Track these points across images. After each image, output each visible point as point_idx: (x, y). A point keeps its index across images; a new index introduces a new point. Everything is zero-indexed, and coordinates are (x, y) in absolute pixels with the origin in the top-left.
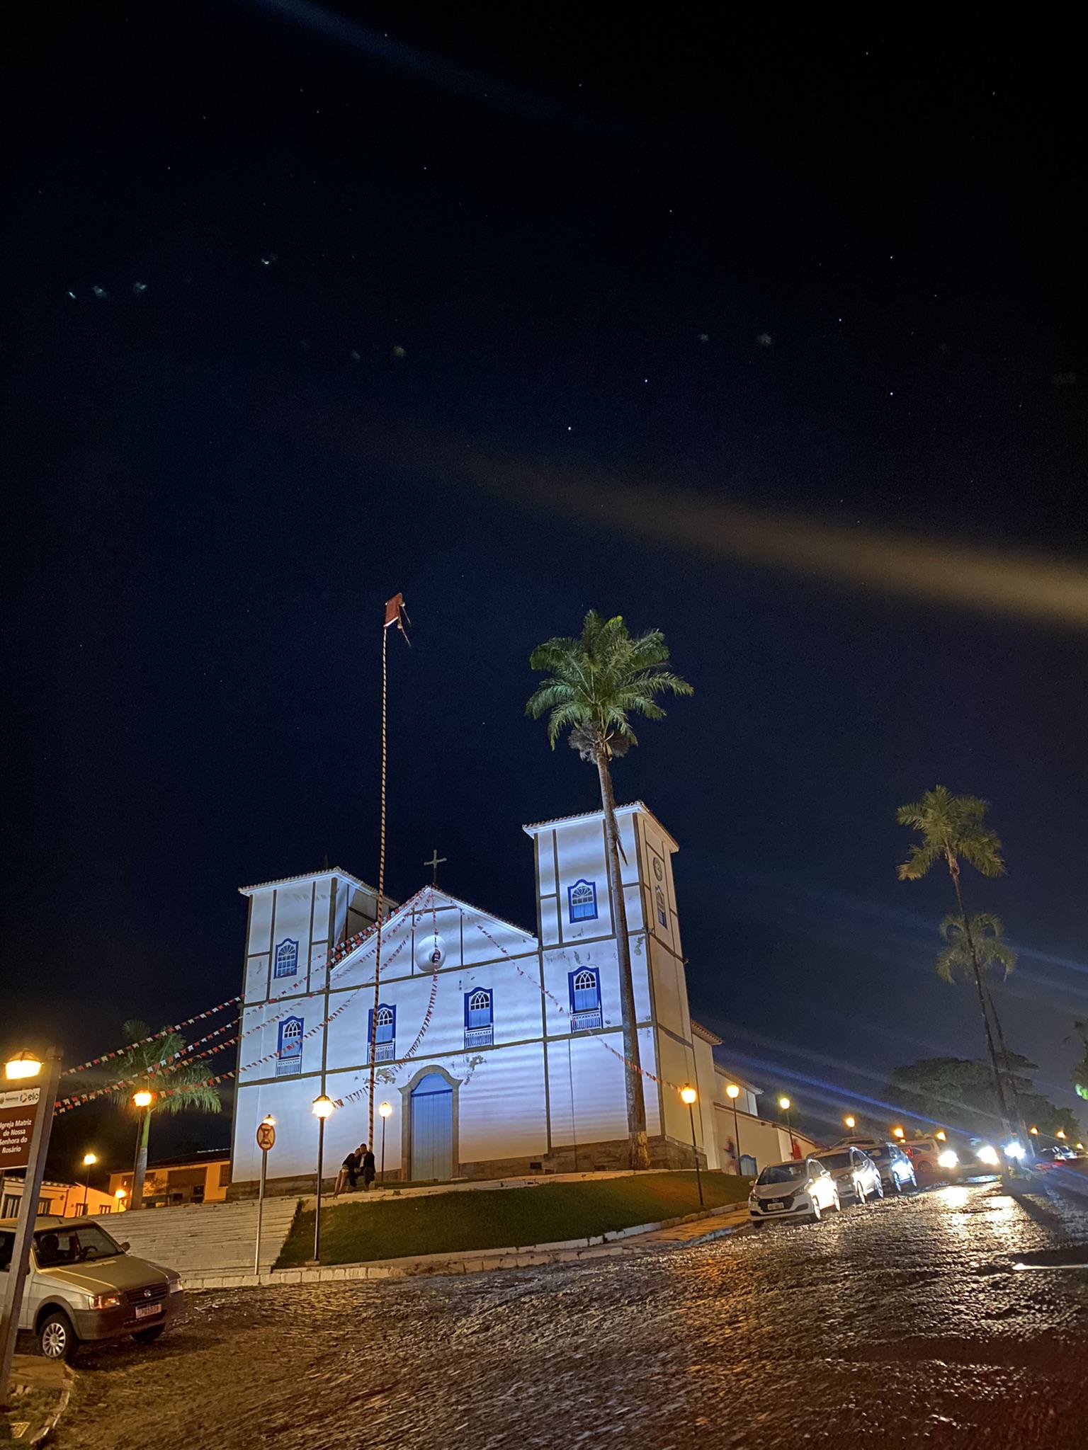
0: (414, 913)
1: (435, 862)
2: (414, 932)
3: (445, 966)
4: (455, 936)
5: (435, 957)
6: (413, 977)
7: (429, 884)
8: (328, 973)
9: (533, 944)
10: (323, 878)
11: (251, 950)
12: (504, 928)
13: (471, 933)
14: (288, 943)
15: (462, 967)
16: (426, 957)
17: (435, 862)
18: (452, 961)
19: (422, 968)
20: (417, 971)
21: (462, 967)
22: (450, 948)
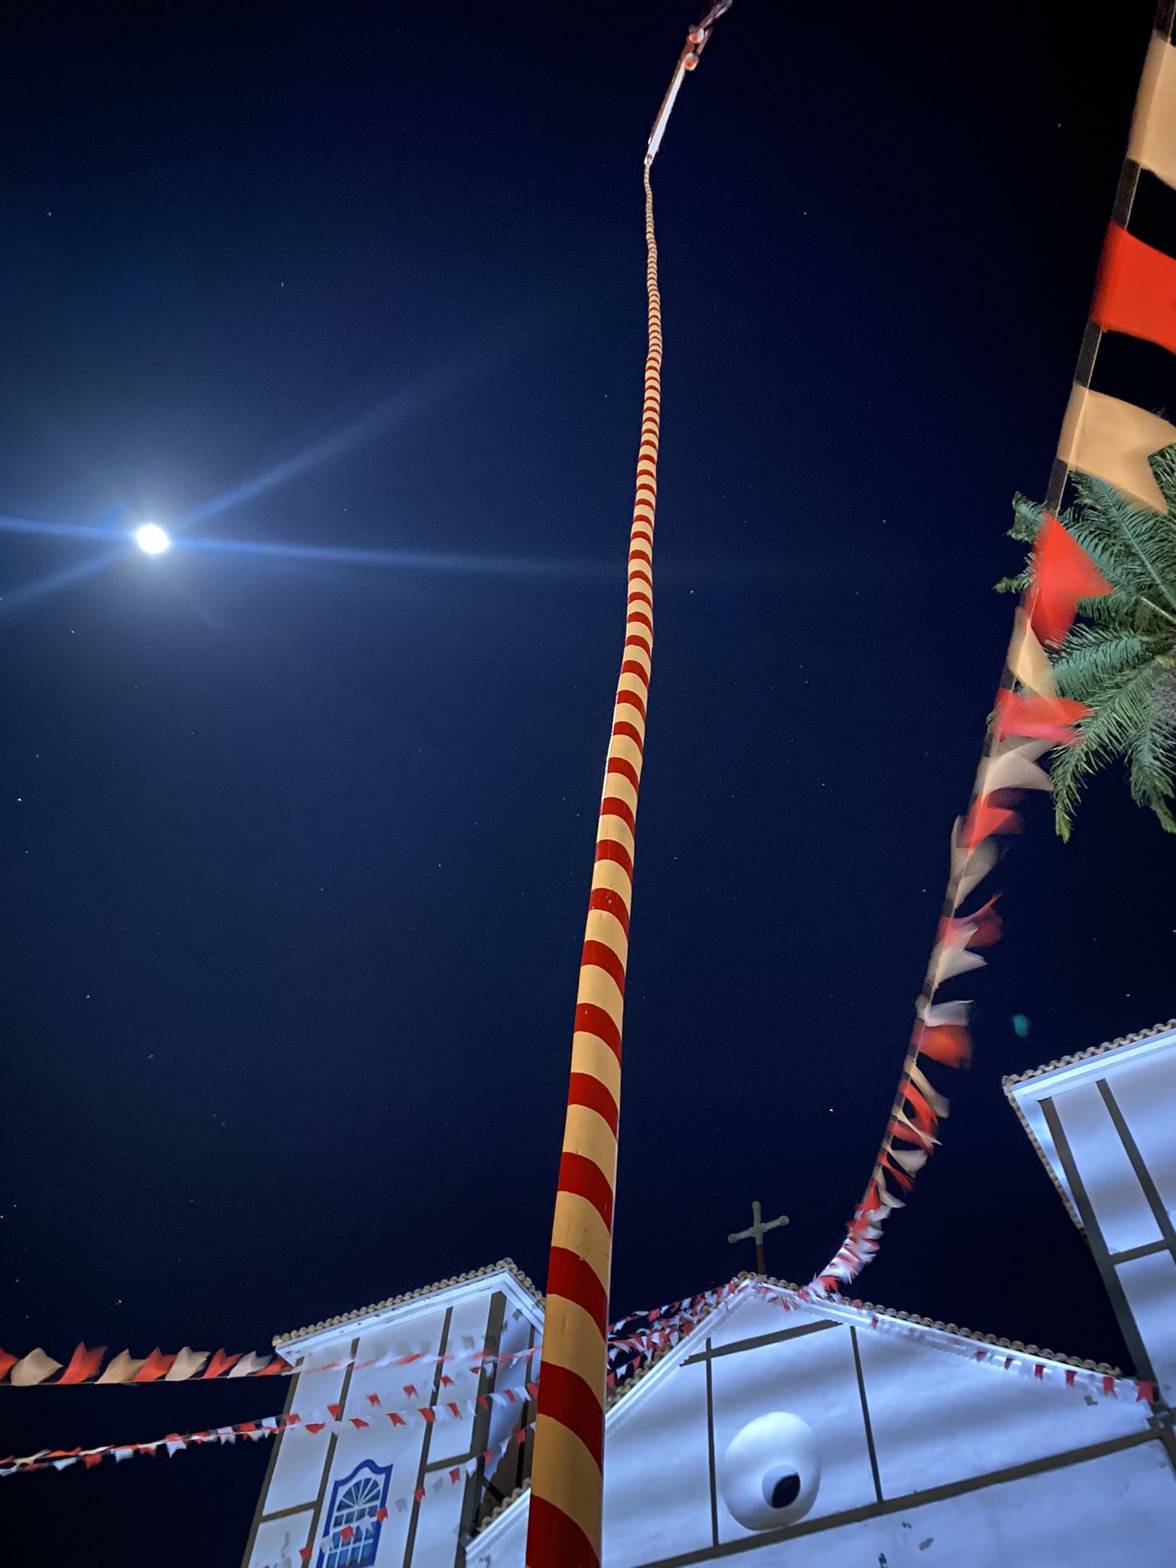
0: (709, 1354)
1: (757, 1230)
2: (711, 1408)
3: (820, 1508)
4: (840, 1407)
5: (786, 1490)
6: (718, 1550)
7: (751, 1268)
8: (461, 1553)
9: (1125, 1409)
10: (470, 1294)
11: (274, 1500)
12: (1005, 1365)
13: (890, 1396)
14: (366, 1473)
15: (880, 1507)
16: (756, 1488)
17: (757, 1230)
18: (843, 1488)
19: (743, 1520)
20: (731, 1529)
21: (880, 1507)
22: (826, 1451)
